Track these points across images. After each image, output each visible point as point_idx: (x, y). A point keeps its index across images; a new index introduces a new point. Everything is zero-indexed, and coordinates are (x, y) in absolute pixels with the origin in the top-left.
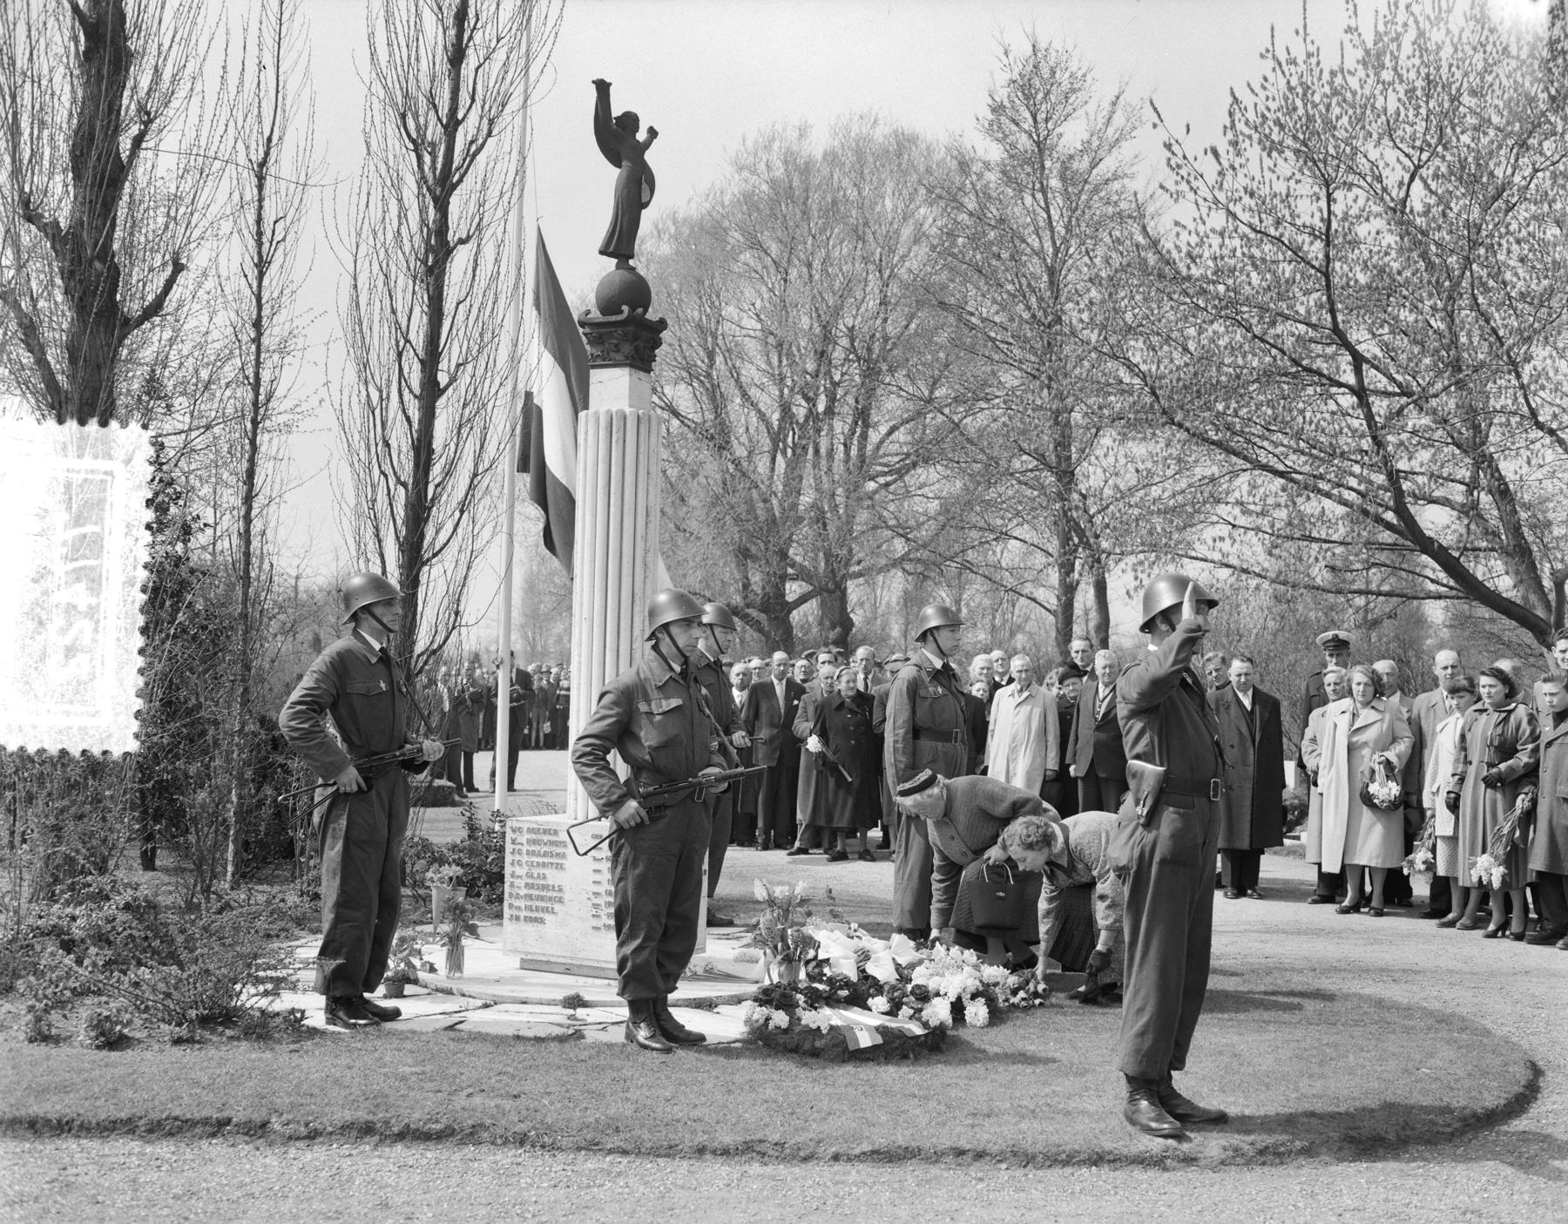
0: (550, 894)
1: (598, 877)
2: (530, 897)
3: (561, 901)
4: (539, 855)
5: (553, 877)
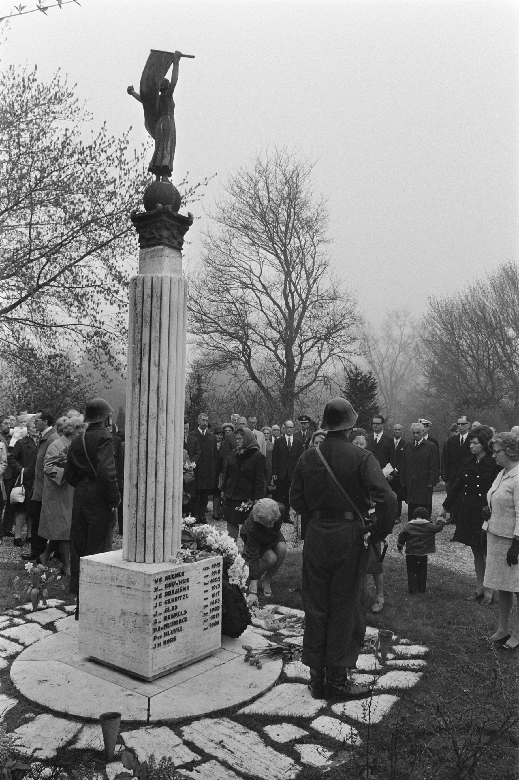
0: (179, 618)
1: (206, 595)
2: (166, 626)
3: (186, 619)
4: (173, 593)
5: (182, 605)
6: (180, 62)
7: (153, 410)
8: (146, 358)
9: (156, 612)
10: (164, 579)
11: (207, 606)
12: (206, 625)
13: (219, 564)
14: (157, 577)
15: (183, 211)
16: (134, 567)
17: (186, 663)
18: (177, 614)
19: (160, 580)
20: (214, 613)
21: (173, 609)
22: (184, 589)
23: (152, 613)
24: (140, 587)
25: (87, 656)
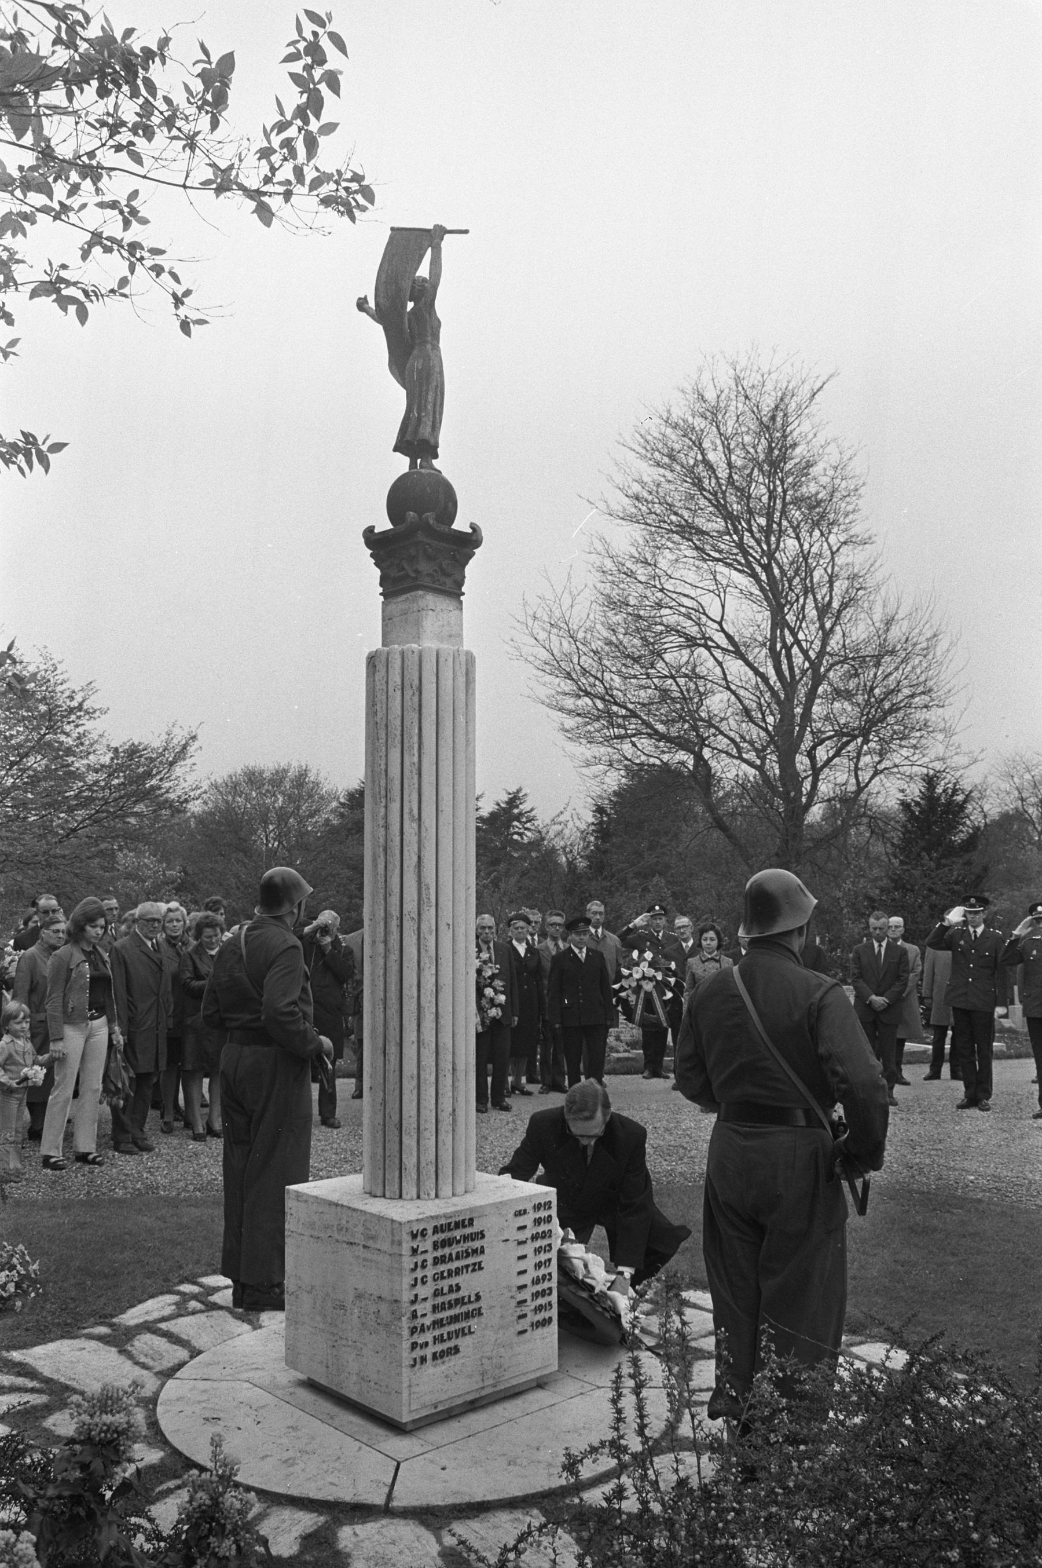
0: (464, 1309)
1: (522, 1265)
2: (438, 1324)
3: (479, 1312)
4: (451, 1259)
5: (469, 1283)
6: (444, 244)
7: (410, 906)
8: (395, 806)
9: (416, 1296)
10: (430, 1231)
11: (525, 1286)
12: (524, 1324)
13: (548, 1205)
14: (417, 1227)
15: (461, 524)
16: (377, 1206)
17: (481, 1398)
18: (460, 1302)
19: (423, 1233)
20: (541, 1301)
21: (451, 1290)
22: (475, 1251)
23: (407, 1296)
24: (385, 1246)
25: (302, 1377)
